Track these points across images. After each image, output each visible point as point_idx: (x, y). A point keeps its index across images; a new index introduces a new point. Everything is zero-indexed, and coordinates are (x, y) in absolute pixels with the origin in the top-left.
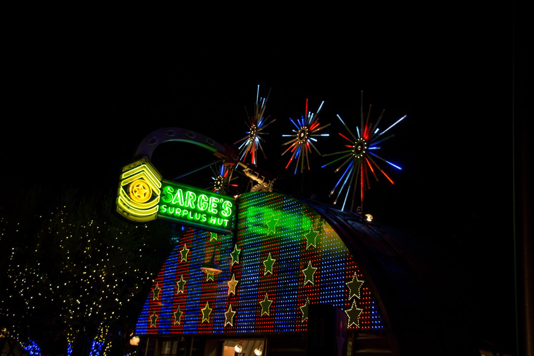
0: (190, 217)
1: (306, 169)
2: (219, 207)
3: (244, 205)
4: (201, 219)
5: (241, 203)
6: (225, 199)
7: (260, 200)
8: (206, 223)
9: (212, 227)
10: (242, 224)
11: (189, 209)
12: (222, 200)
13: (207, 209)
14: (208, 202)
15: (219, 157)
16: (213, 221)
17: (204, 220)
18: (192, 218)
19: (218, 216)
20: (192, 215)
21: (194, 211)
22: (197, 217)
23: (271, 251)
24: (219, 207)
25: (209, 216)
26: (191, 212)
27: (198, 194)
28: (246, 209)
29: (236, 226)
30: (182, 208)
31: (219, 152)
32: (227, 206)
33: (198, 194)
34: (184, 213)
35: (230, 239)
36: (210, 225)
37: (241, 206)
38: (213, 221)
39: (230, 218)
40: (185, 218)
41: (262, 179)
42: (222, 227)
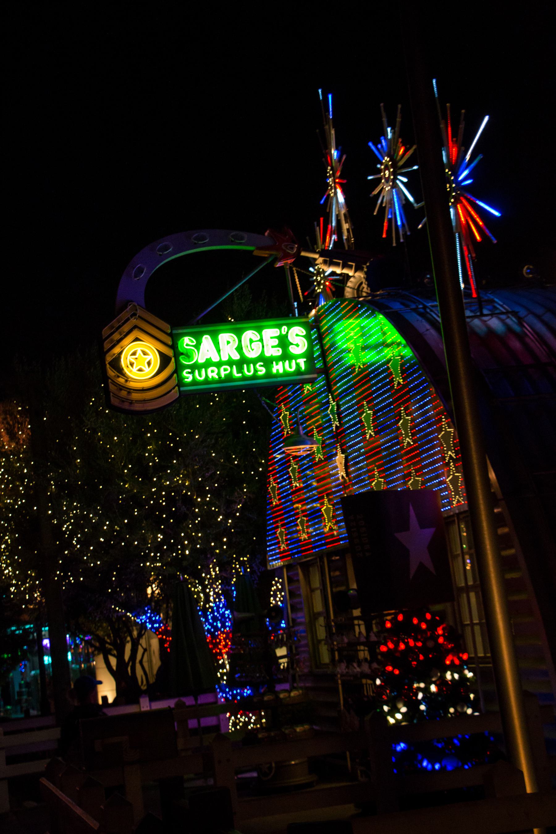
0: (236, 375)
1: (405, 235)
2: (283, 342)
3: (325, 325)
4: (256, 371)
5: (321, 322)
6: (289, 326)
7: (338, 313)
8: (268, 375)
9: (279, 379)
10: (332, 357)
11: (230, 363)
12: (284, 329)
13: (263, 352)
14: (261, 340)
15: (266, 256)
16: (277, 370)
17: (262, 371)
18: (240, 375)
19: (286, 357)
20: (240, 370)
21: (242, 362)
22: (248, 371)
23: (364, 398)
24: (283, 342)
25: (267, 362)
26: (234, 367)
27: (238, 332)
28: (330, 329)
29: (325, 363)
30: (219, 365)
31: (259, 248)
32: (298, 337)
33: (238, 332)
34: (224, 372)
35: (323, 386)
36: (275, 376)
37: (322, 327)
38: (278, 368)
39: (309, 356)
40: (229, 378)
41: (350, 267)
42: (298, 372)
